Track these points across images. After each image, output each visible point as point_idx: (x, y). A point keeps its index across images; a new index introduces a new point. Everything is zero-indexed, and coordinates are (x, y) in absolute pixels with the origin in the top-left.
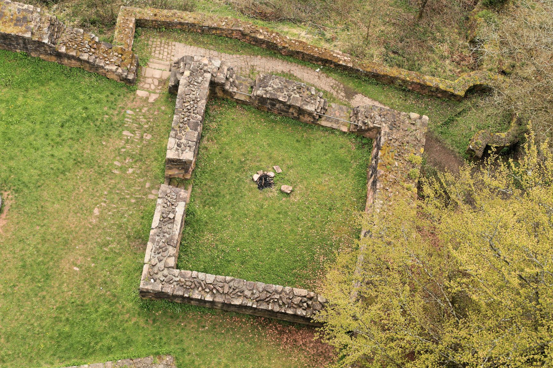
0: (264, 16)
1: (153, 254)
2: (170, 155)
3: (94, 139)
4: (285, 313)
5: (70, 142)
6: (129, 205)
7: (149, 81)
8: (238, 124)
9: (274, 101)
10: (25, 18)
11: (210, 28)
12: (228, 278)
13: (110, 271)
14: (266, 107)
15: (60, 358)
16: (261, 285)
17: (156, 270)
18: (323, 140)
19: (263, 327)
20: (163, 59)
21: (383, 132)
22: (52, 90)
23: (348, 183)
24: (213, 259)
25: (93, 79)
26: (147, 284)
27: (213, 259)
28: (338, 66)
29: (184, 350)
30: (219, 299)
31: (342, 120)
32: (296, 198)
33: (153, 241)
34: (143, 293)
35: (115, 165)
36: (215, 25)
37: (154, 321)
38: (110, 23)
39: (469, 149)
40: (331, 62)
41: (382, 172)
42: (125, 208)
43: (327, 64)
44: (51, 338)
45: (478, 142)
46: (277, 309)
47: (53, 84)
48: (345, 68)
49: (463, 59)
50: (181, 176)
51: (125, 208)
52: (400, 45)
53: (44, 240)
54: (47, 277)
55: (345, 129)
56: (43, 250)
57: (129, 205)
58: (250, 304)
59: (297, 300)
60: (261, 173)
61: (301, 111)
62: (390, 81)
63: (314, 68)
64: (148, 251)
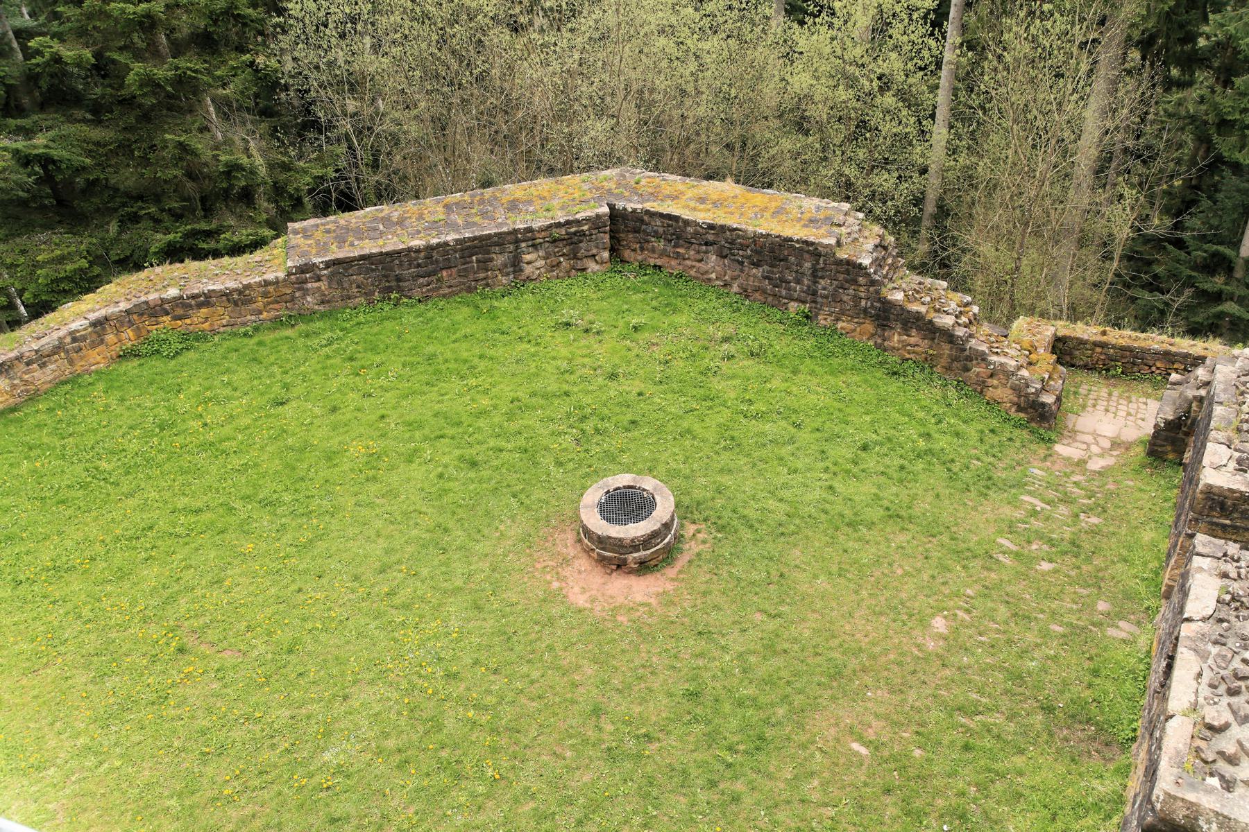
1: (1205, 691)
6: (1045, 634)
13: (982, 787)
25: (952, 393)
26: (1192, 787)
35: (1002, 546)
51: (1030, 638)
53: (771, 649)
56: (762, 671)
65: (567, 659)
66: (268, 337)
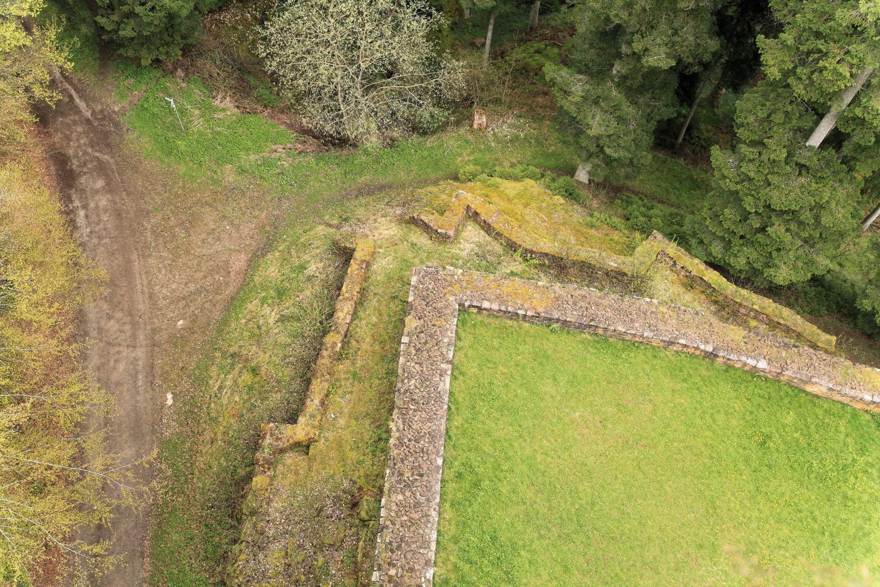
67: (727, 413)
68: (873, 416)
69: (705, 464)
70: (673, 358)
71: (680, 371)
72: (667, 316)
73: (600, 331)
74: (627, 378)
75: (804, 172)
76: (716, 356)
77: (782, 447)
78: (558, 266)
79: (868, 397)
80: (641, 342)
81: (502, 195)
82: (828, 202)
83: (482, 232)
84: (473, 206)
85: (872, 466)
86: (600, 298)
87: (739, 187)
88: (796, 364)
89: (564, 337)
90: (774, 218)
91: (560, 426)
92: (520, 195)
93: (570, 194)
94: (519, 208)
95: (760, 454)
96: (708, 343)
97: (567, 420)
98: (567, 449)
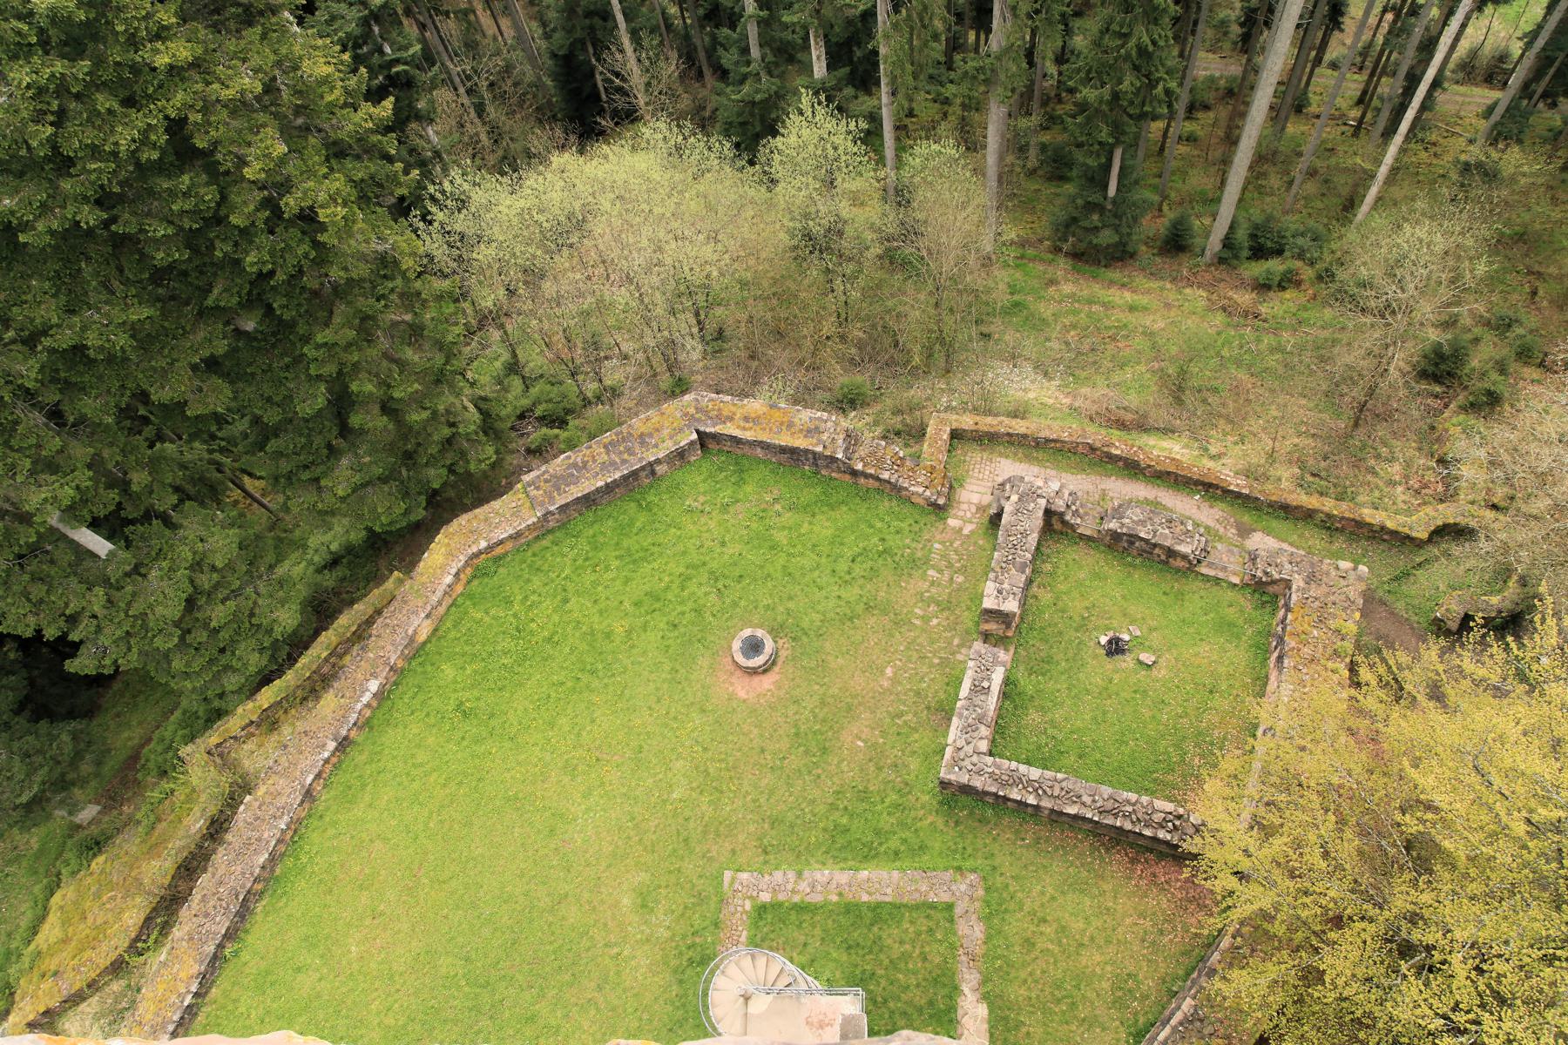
0: (1121, 425)
2: (988, 603)
3: (891, 579)
4: (1140, 834)
5: (861, 581)
6: (931, 666)
7: (965, 507)
8: (1081, 568)
9: (1133, 538)
10: (817, 428)
11: (1048, 441)
12: (1060, 776)
14: (1121, 545)
15: (835, 857)
16: (1106, 791)
17: (962, 754)
18: (1202, 593)
19: (1107, 850)
20: (983, 480)
21: (1294, 587)
22: (844, 516)
23: (1238, 656)
24: (1039, 748)
25: (894, 503)
27: (1039, 748)
28: (1226, 492)
29: (994, 868)
30: (1046, 803)
31: (1231, 567)
32: (1161, 673)
33: (960, 716)
34: (944, 784)
36: (1054, 436)
37: (957, 823)
38: (916, 434)
39: (1436, 619)
40: (1217, 487)
41: (1293, 644)
42: (925, 669)
43: (1210, 489)
44: (825, 830)
45: (1452, 608)
46: (1128, 826)
47: (845, 509)
48: (1238, 495)
49: (1426, 486)
50: (1001, 633)
51: (925, 669)
52: (1323, 464)
53: (823, 703)
54: (824, 750)
55: (1236, 580)
56: (821, 716)
57: (931, 666)
58: (1089, 815)
59: (1158, 817)
60: (1111, 634)
61: (1171, 553)
62: (1306, 515)
63: (1194, 492)
64: (953, 729)
65: (746, 728)
66: (536, 547)
67: (418, 746)
68: (475, 577)
69: (465, 795)
70: (332, 793)
71: (350, 788)
72: (272, 789)
73: (259, 887)
74: (332, 865)
75: (143, 571)
76: (346, 738)
77: (476, 693)
78: (168, 905)
79: (449, 579)
80: (295, 831)
81: (52, 951)
82: (195, 553)
83: (83, 1006)
84: (31, 1017)
85: (526, 598)
86: (214, 875)
87: (135, 650)
88: (387, 646)
89: (250, 939)
90: (199, 615)
91: (361, 978)
92: (66, 922)
93: (98, 843)
94: (83, 930)
95: (475, 722)
96: (324, 745)
97: (355, 966)
98: (391, 978)
